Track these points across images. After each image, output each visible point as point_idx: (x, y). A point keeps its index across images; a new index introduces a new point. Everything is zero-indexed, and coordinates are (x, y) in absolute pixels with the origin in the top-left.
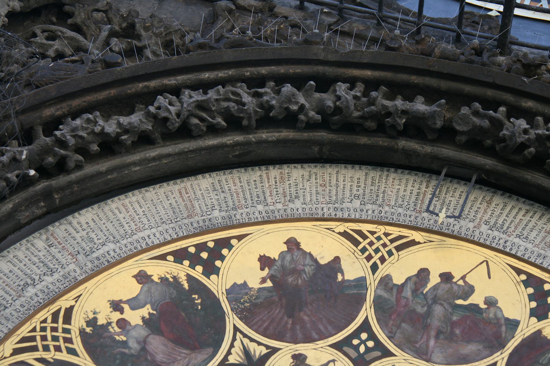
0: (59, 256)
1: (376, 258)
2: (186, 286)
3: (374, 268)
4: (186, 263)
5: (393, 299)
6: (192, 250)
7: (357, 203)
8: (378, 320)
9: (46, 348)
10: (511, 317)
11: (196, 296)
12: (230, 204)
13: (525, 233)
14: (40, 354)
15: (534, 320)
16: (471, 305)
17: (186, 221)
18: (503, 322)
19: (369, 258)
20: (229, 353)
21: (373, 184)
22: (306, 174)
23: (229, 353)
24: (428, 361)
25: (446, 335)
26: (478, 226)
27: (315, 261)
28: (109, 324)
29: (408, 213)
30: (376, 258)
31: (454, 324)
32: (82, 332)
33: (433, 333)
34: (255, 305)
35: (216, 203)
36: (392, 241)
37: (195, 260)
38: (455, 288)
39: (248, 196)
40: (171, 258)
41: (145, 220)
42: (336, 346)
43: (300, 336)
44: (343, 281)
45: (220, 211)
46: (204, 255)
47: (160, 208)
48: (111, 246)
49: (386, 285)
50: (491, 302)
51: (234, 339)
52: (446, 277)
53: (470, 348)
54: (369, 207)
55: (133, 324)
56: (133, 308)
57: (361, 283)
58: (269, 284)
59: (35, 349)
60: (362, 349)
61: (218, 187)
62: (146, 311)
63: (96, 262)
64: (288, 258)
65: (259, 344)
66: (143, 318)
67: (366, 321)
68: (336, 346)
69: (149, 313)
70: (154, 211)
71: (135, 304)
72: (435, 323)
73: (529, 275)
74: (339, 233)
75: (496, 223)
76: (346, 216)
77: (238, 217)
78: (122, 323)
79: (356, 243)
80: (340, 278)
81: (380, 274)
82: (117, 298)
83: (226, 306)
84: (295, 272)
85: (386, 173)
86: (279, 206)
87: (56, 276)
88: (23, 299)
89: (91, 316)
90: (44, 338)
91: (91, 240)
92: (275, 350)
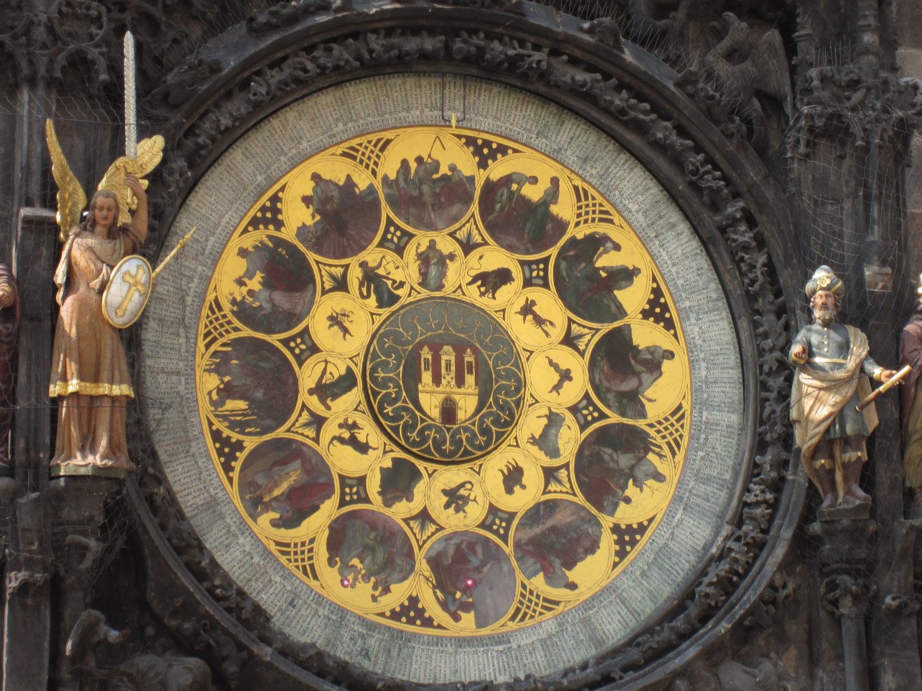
0: (187, 264)
1: (372, 165)
2: (271, 245)
3: (374, 173)
4: (261, 227)
5: (396, 192)
6: (259, 215)
7: (341, 125)
8: (395, 213)
9: (221, 335)
10: (468, 175)
11: (280, 250)
12: (263, 165)
13: (452, 104)
14: (221, 341)
15: (482, 170)
16: (442, 176)
17: (245, 194)
18: (465, 180)
19: (367, 166)
20: (323, 283)
21: (343, 104)
22: (296, 114)
23: (323, 283)
24: (436, 230)
25: (438, 206)
26: (422, 112)
27: (336, 185)
28: (244, 298)
29: (376, 119)
30: (372, 165)
31: (438, 196)
32: (233, 312)
33: (430, 208)
34: (318, 238)
35: (254, 169)
36: (375, 146)
37: (266, 222)
38: (428, 166)
39: (270, 152)
40: (250, 228)
41: (219, 207)
42: (381, 245)
43: (356, 248)
44: (361, 192)
45: (261, 174)
46: (269, 215)
47: (222, 191)
48: (212, 240)
49: (387, 183)
50: (453, 168)
51: (320, 271)
52: (419, 160)
53: (456, 208)
54: (350, 125)
55: (257, 290)
56: (251, 278)
57: (371, 189)
58: (318, 217)
59: (214, 340)
60: (395, 240)
61: (248, 155)
62: (259, 277)
63: (212, 257)
64: (319, 190)
65: (336, 266)
66: (260, 283)
67: (388, 218)
68: (381, 245)
69: (262, 277)
70: (220, 196)
71: (250, 274)
72: (428, 199)
73: (467, 137)
74: (341, 155)
75: (432, 104)
76: (339, 140)
77: (274, 174)
78: (251, 293)
79: (354, 158)
80: (357, 191)
81: (380, 176)
82: (237, 277)
83: (302, 247)
84: (329, 199)
85: (345, 89)
86: (294, 151)
87: (196, 281)
88: (188, 308)
89: (231, 298)
90: (215, 329)
91: (197, 241)
92: (347, 267)
